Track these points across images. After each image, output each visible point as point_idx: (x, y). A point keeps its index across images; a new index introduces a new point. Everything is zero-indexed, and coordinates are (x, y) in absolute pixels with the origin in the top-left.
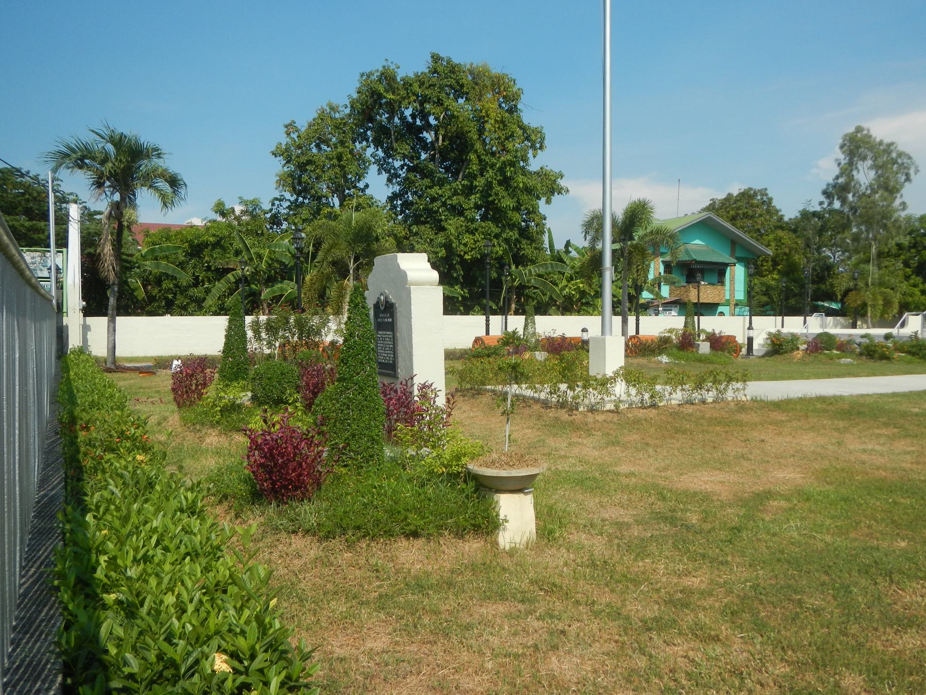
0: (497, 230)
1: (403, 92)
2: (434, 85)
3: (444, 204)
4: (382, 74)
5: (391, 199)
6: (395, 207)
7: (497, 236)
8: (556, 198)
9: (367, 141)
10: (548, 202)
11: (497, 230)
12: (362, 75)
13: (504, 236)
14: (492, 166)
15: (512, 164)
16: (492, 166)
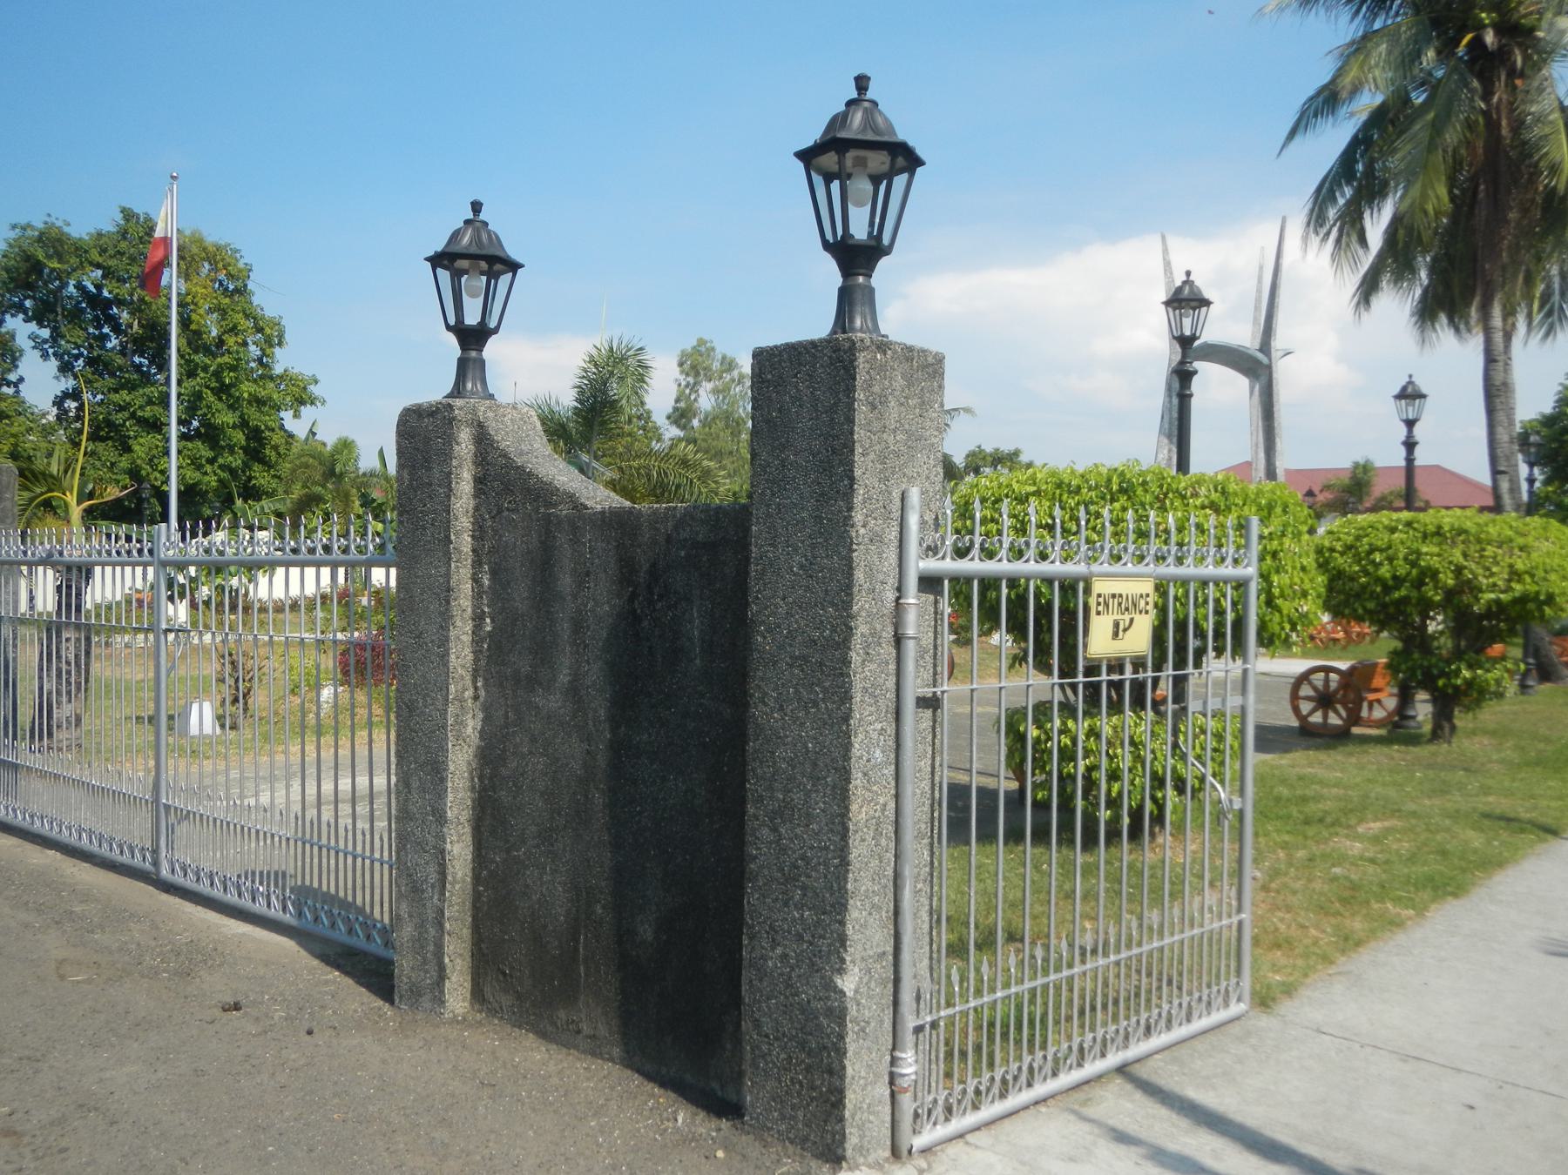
0: (210, 454)
1: (74, 261)
2: (122, 254)
3: (133, 415)
4: (42, 234)
5: (59, 402)
6: (66, 412)
7: (211, 461)
8: (306, 411)
9: (25, 313)
10: (297, 415)
11: (210, 454)
12: (14, 227)
13: (220, 461)
14: (205, 369)
15: (233, 368)
16: (205, 369)
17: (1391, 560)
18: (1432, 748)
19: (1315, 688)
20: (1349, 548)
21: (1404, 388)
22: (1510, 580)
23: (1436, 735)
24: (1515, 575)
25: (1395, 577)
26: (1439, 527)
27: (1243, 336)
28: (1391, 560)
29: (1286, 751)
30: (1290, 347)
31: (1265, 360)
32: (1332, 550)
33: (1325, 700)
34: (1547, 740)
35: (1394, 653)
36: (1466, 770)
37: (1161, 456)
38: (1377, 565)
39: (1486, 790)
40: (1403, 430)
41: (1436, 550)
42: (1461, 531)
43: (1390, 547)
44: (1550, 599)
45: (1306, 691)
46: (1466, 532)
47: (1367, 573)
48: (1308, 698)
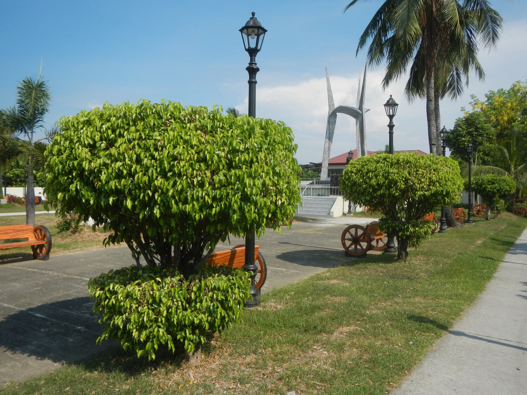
17: (376, 176)
18: (397, 264)
19: (351, 235)
20: (359, 171)
21: (388, 101)
22: (429, 185)
23: (399, 258)
24: (432, 182)
25: (378, 184)
26: (398, 160)
27: (354, 104)
28: (376, 176)
29: (334, 267)
30: (369, 108)
31: (361, 112)
32: (352, 172)
33: (356, 240)
34: (448, 257)
35: (382, 220)
36: (409, 278)
37: (326, 146)
38: (370, 179)
39: (416, 293)
40: (388, 120)
41: (396, 171)
42: (408, 162)
43: (376, 170)
44: (448, 193)
45: (348, 236)
46: (410, 162)
47: (366, 183)
48: (348, 239)
